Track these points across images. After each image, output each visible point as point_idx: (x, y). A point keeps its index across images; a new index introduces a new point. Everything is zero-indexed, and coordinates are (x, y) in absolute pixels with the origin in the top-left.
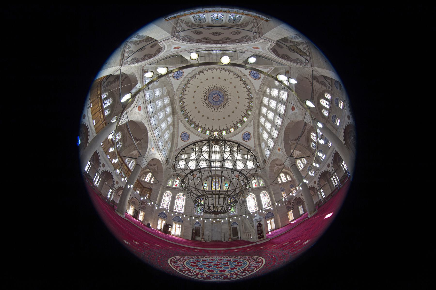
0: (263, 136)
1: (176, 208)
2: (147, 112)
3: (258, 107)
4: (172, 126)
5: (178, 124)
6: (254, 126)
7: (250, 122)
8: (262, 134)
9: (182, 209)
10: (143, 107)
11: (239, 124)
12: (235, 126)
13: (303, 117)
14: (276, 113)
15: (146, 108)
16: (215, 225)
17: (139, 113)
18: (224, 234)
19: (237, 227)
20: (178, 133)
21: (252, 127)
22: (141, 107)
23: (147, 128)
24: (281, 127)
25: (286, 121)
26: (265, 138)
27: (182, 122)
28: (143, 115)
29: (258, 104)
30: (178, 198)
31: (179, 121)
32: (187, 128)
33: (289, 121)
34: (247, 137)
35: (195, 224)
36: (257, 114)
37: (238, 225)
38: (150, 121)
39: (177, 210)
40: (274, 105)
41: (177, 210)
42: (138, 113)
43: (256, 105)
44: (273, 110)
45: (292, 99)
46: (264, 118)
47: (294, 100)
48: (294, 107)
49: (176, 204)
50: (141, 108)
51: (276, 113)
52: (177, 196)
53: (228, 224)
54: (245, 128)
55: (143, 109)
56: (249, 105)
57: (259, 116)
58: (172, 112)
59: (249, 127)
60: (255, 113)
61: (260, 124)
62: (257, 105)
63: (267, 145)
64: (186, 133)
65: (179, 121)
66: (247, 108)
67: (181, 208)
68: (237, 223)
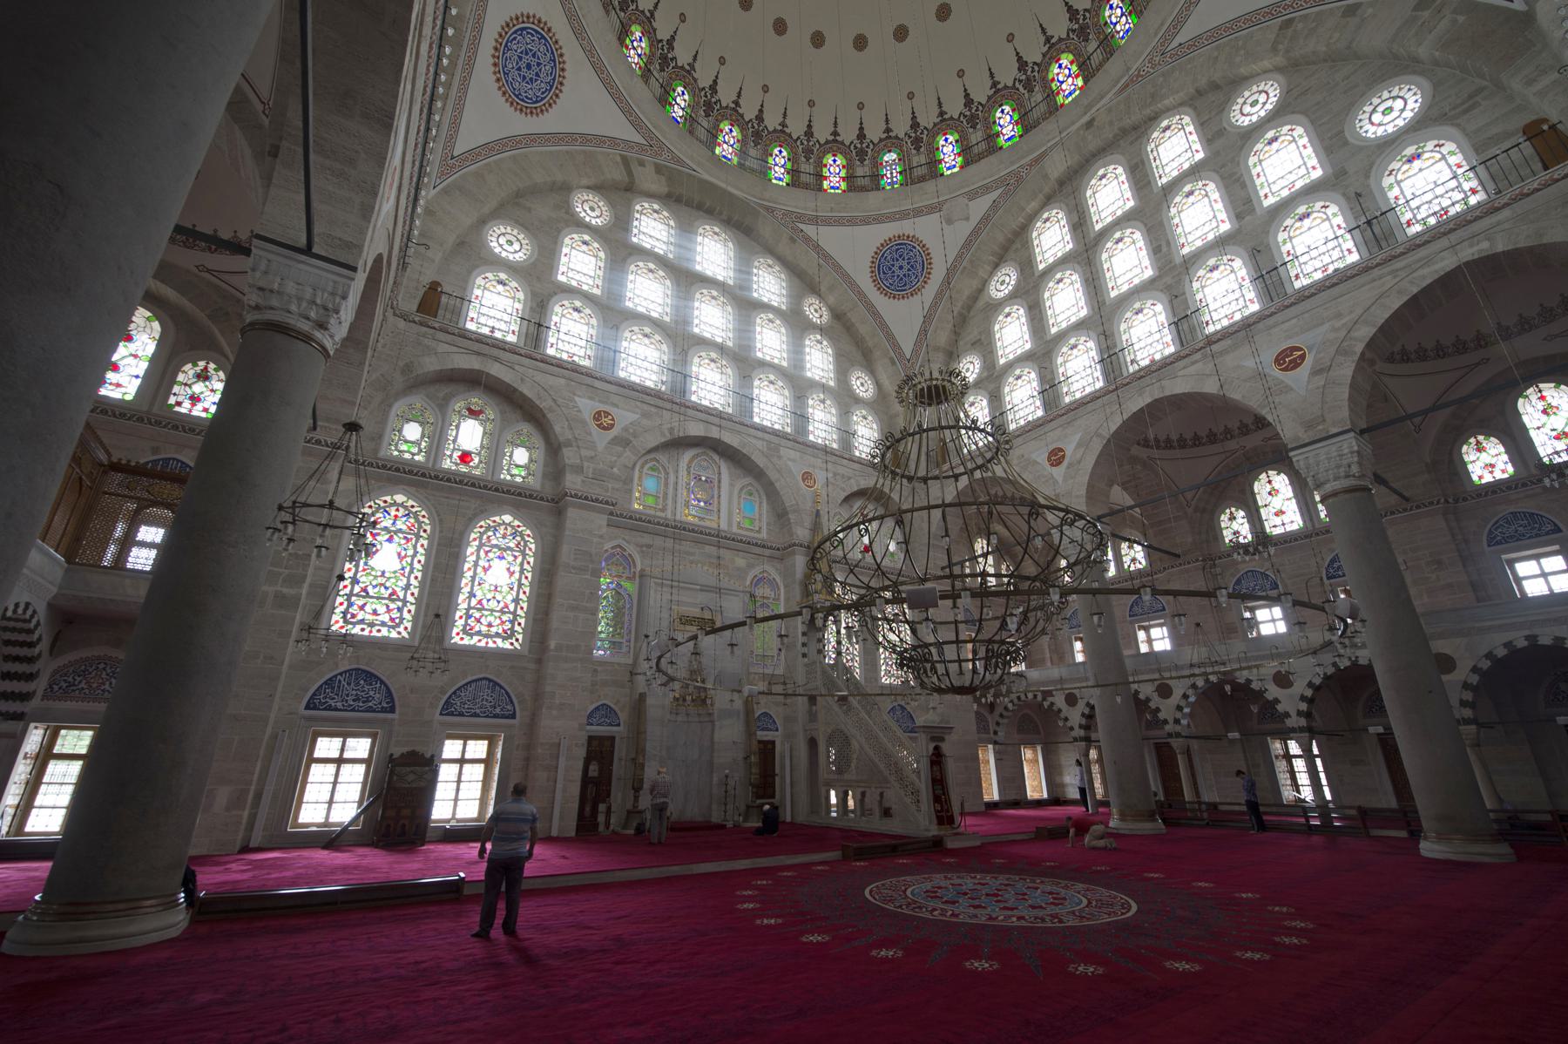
0: (997, 327)
1: (471, 622)
3: (1093, 143)
6: (976, 232)
7: (973, 195)
8: (996, 307)
9: (512, 622)
11: (890, 157)
12: (862, 154)
13: (1306, 438)
14: (1168, 280)
16: (680, 718)
18: (727, 776)
19: (773, 743)
21: (963, 230)
24: (1142, 377)
25: (1192, 370)
26: (999, 344)
29: (1111, 123)
30: (487, 553)
33: (1210, 387)
34: (901, 268)
35: (590, 716)
36: (1046, 177)
37: (777, 730)
40: (1199, 233)
41: (479, 633)
43: (1086, 118)
44: (1164, 249)
45: (1339, 316)
46: (1068, 238)
47: (1343, 333)
48: (1303, 357)
49: (472, 595)
51: (1168, 280)
52: (473, 536)
53: (742, 716)
54: (918, 213)
56: (1043, 67)
57: (1048, 202)
59: (949, 222)
60: (1037, 160)
61: (1018, 245)
62: (1090, 124)
63: (992, 386)
66: (1008, 74)
67: (505, 618)
68: (774, 721)
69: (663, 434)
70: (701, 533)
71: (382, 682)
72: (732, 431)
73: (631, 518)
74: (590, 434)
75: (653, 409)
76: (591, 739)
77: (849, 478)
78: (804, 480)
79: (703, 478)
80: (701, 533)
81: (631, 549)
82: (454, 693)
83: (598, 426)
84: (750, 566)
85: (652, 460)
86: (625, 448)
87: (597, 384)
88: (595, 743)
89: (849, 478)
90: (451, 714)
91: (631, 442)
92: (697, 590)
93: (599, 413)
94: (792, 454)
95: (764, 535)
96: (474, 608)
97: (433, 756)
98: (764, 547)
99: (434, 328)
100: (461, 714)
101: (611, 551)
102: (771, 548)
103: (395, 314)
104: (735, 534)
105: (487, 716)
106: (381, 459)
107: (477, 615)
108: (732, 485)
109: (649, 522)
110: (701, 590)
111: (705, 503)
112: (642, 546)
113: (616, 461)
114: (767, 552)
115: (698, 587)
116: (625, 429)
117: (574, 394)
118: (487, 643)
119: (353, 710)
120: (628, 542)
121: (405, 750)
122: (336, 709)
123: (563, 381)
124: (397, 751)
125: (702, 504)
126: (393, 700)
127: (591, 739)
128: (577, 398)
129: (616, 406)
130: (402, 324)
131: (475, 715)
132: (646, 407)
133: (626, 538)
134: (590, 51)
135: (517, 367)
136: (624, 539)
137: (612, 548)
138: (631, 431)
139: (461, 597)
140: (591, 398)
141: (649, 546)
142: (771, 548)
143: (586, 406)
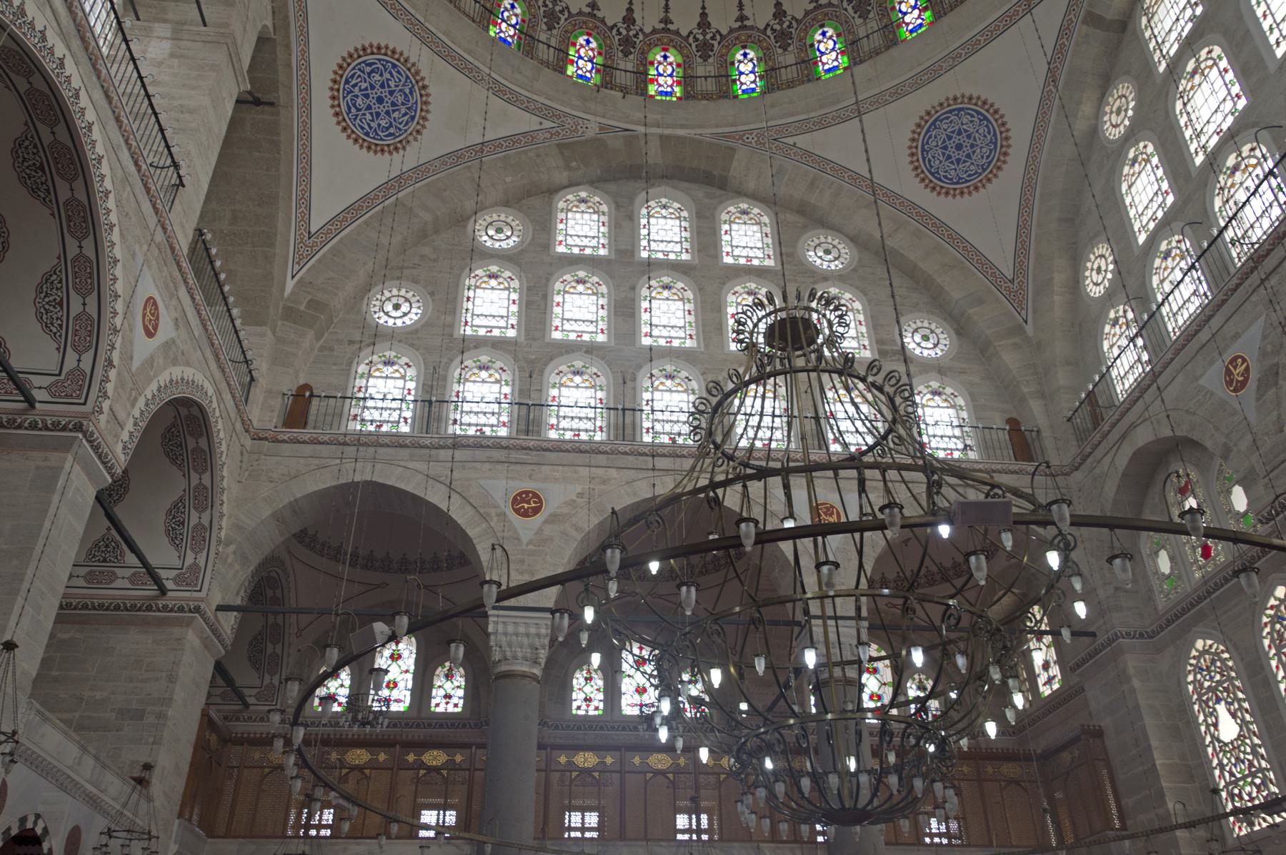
2: (581, 452)
4: (805, 228)
5: (823, 163)
10: (530, 477)
15: (547, 454)
17: (554, 519)
22: (520, 494)
27: (822, 124)
28: (579, 490)
31: (802, 141)
32: (898, 93)
42: (548, 531)
50: (527, 493)
58: (700, 192)
64: (930, 122)
65: (802, 141)
86: (1276, 384)
87: (1204, 335)
91: (1277, 365)
93: (1229, 372)
99: (1090, 454)
103: (1068, 474)
106: (1163, 615)
113: (1279, 416)
116: (1263, 354)
117: (1197, 379)
123: (1180, 378)
128: (1202, 382)
129: (1236, 336)
130: (1078, 476)
134: (954, 59)
138: (1269, 348)
140: (1212, 362)
143: (1212, 378)
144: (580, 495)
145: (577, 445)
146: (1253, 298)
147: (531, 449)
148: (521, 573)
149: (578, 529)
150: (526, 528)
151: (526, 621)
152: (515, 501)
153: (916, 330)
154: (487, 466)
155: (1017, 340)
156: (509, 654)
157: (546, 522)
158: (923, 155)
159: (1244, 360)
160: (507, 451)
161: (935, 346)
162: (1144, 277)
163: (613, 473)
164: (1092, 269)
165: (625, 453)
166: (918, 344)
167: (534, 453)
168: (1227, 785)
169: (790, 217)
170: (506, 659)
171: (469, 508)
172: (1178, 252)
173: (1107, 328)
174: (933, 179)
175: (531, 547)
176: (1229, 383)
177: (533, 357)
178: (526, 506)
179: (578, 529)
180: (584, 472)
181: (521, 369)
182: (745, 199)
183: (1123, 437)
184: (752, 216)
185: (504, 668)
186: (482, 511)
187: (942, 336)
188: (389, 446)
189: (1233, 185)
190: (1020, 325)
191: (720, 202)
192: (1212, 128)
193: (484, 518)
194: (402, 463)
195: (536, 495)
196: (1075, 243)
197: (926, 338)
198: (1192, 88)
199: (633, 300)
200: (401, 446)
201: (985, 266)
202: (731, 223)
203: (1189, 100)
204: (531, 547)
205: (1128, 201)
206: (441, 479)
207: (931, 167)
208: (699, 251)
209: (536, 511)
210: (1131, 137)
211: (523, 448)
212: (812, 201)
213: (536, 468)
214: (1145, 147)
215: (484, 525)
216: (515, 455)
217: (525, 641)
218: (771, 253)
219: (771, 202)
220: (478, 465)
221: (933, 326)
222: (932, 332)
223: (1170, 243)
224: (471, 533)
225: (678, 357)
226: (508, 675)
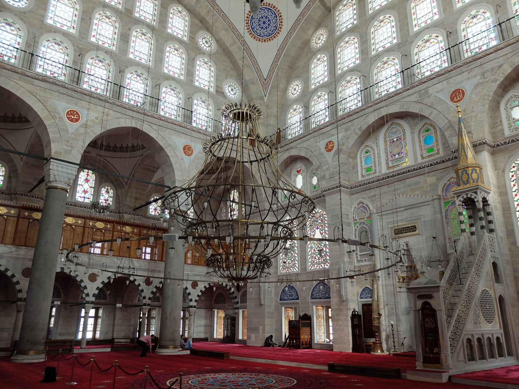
2: (100, 99)
4: (201, 28)
10: (76, 104)
20: (234, 30)
22: (70, 111)
23: (134, 125)
38: (124, 108)
39: (316, 264)
41: (316, 264)
50: (74, 111)
55: (83, 107)
69: (357, 134)
70: (399, 174)
71: (295, 289)
72: (392, 103)
73: (360, 185)
74: (325, 158)
75: (350, 124)
76: (364, 305)
77: (500, 66)
78: (452, 99)
79: (395, 140)
80: (399, 174)
81: (367, 202)
82: (313, 290)
83: (328, 151)
84: (439, 179)
85: (365, 148)
87: (324, 130)
88: (365, 307)
89: (500, 66)
90: (313, 298)
92: (402, 211)
93: (327, 145)
94: (439, 86)
95: (442, 154)
96: (313, 253)
97: (310, 316)
98: (443, 162)
100: (316, 298)
101: (357, 207)
102: (449, 160)
104: (419, 164)
105: (324, 298)
107: (314, 256)
108: (413, 133)
109: (369, 183)
110: (405, 210)
111: (398, 154)
112: (371, 197)
114: (449, 164)
115: (403, 209)
117: (317, 142)
118: (319, 267)
119: (289, 300)
120: (365, 199)
121: (303, 313)
122: (286, 300)
123: (312, 140)
124: (302, 314)
125: (397, 156)
126: (298, 296)
127: (364, 305)
131: (320, 298)
132: (345, 125)
133: (363, 196)
135: (298, 146)
136: (362, 198)
137: (358, 205)
139: (309, 249)
140: (323, 139)
141: (375, 196)
142: (449, 160)
143: (322, 144)
144: (96, 118)
145: (99, 96)
146: (342, 126)
147: (78, 92)
148: (68, 146)
149: (94, 133)
150: (72, 127)
151: (67, 167)
152: (68, 113)
153: (230, 86)
154: (57, 94)
155: (261, 102)
156: (57, 179)
157: (80, 126)
158: (251, 19)
159: (333, 143)
160: (67, 90)
161: (235, 94)
162: (310, 100)
163: (111, 112)
164: (293, 88)
165: (118, 106)
166: (229, 92)
167: (79, 94)
168: (283, 259)
169: (197, 22)
170: (56, 181)
171: (46, 111)
172: (323, 98)
173: (291, 111)
174: (252, 30)
175: (73, 136)
176: (326, 148)
177: (81, 47)
178: (73, 117)
179: (94, 133)
180: (101, 109)
181: (75, 51)
182: (180, 5)
183: (287, 150)
184: (182, 14)
185: (54, 184)
186: (52, 114)
187: (237, 91)
188: (9, 70)
189: (346, 86)
190: (263, 97)
191: (171, 3)
192: (347, 64)
193: (54, 117)
194: (15, 80)
195: (77, 113)
196: (290, 76)
197: (232, 90)
198: (345, 47)
199: (129, 35)
200: (16, 72)
201: (258, 70)
202: (174, 14)
203: (342, 50)
204: (73, 136)
205: (312, 71)
206: (34, 94)
207: (252, 25)
208: (159, 22)
209: (77, 120)
210: (319, 50)
211: (75, 91)
212: (207, 19)
213: (79, 101)
214: (324, 57)
215: (53, 121)
216: (70, 92)
217: (66, 175)
218: (186, 35)
219: (191, 11)
220: (53, 92)
221: (235, 86)
222: (235, 88)
223: (321, 94)
224: (46, 123)
225: (143, 68)
226: (56, 188)
